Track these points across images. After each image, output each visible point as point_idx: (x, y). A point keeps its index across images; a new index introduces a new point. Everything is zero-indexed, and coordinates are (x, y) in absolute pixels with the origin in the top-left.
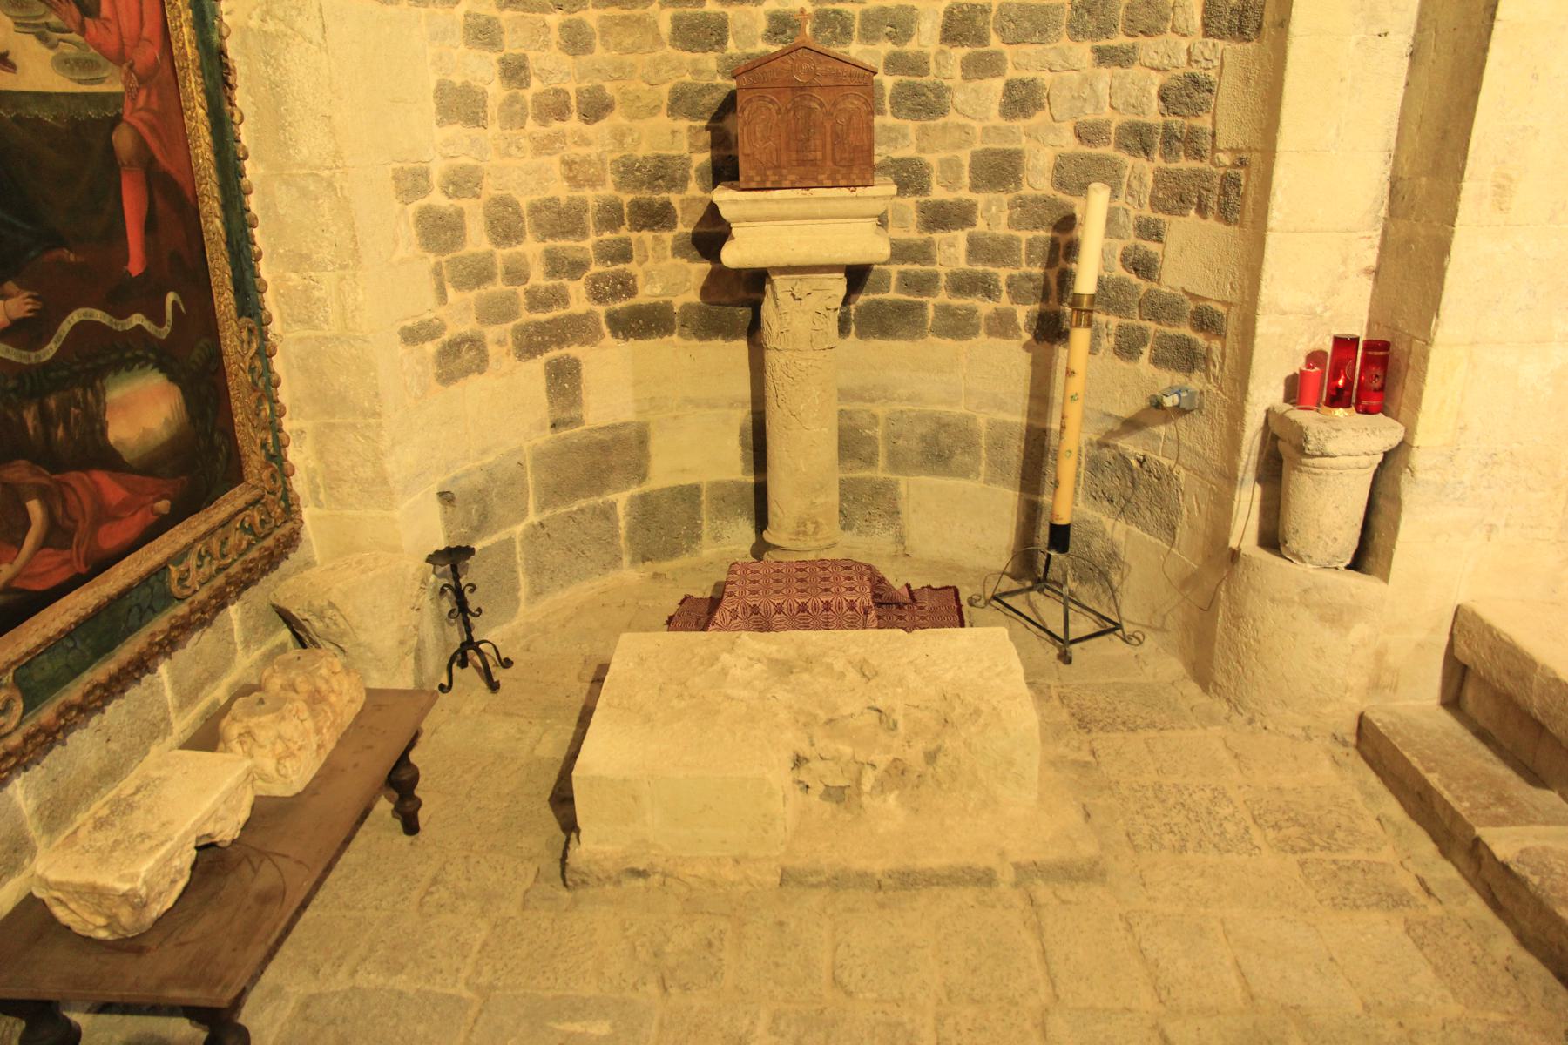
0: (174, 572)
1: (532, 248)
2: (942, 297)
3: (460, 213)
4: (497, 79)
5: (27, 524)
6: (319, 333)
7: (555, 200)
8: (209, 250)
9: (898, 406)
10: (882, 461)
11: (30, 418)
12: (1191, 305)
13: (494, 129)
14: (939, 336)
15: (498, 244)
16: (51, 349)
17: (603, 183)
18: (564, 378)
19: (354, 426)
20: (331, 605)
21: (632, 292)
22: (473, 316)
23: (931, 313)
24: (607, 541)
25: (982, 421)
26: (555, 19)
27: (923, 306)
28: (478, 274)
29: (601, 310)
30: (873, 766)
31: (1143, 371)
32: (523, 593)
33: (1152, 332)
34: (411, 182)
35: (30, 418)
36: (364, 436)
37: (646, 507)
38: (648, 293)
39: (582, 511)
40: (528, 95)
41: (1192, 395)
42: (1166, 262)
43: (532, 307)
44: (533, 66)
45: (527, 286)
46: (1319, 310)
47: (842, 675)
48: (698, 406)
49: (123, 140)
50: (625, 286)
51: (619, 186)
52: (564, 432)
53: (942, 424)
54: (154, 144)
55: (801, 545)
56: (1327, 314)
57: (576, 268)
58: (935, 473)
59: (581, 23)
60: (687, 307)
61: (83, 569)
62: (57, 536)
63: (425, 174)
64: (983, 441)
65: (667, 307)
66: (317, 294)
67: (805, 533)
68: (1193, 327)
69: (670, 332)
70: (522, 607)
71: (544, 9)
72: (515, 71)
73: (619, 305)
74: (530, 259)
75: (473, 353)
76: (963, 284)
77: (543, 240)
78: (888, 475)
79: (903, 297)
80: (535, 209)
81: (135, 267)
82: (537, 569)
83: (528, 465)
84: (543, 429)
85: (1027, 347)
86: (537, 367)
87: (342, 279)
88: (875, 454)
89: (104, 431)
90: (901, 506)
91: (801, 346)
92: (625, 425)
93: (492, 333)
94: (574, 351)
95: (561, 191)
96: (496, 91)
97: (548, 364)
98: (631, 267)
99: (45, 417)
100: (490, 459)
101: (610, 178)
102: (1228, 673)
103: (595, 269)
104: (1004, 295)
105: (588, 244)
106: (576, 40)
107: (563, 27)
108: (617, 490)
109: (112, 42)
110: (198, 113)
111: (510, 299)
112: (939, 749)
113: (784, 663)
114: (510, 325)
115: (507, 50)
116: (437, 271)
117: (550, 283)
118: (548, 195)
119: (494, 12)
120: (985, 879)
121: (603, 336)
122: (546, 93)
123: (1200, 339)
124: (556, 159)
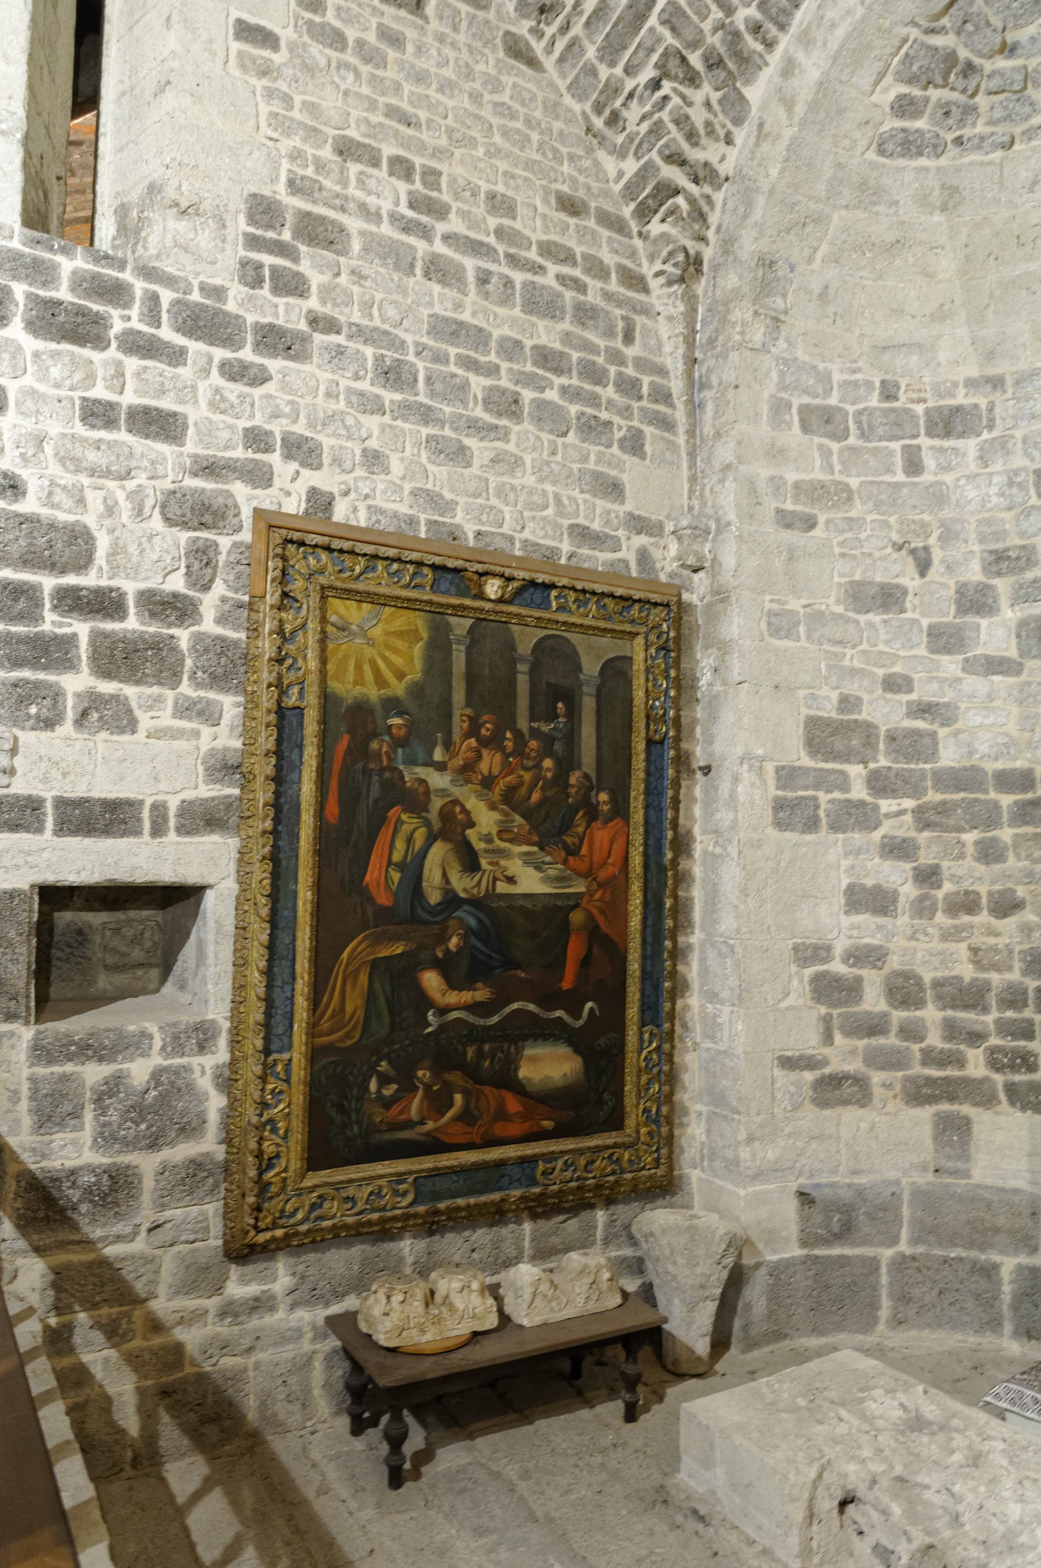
0: (541, 1167)
1: (931, 1014)
3: (859, 980)
4: (910, 882)
5: (451, 1105)
7: (959, 978)
8: (630, 981)
11: (470, 1052)
13: (903, 920)
15: (896, 1008)
16: (495, 1019)
17: (1010, 969)
18: (954, 1132)
24: (989, 1301)
26: (970, 837)
28: (874, 1027)
29: (999, 1079)
34: (811, 953)
35: (470, 1052)
39: (961, 1260)
40: (940, 894)
43: (924, 1063)
44: (945, 874)
49: (577, 917)
51: (1025, 972)
52: (948, 1180)
54: (600, 919)
57: (975, 1037)
59: (995, 840)
61: (478, 1141)
62: (467, 1117)
63: (828, 949)
70: (881, 1327)
71: (960, 830)
72: (928, 876)
73: (1018, 1078)
74: (928, 1024)
80: (937, 984)
81: (566, 984)
82: (902, 1298)
86: (926, 1113)
89: (516, 1070)
92: (1016, 1191)
93: (877, 1077)
94: (966, 1109)
95: (967, 972)
96: (908, 891)
98: (1033, 1046)
99: (479, 1053)
100: (862, 1180)
101: (1017, 965)
103: (994, 1041)
105: (990, 1019)
106: (990, 853)
107: (977, 843)
108: (1002, 1252)
109: (583, 867)
110: (636, 900)
114: (900, 1074)
115: (921, 861)
116: (827, 1020)
117: (947, 1046)
118: (954, 973)
119: (913, 834)
121: (999, 1102)
122: (957, 893)
124: (964, 946)
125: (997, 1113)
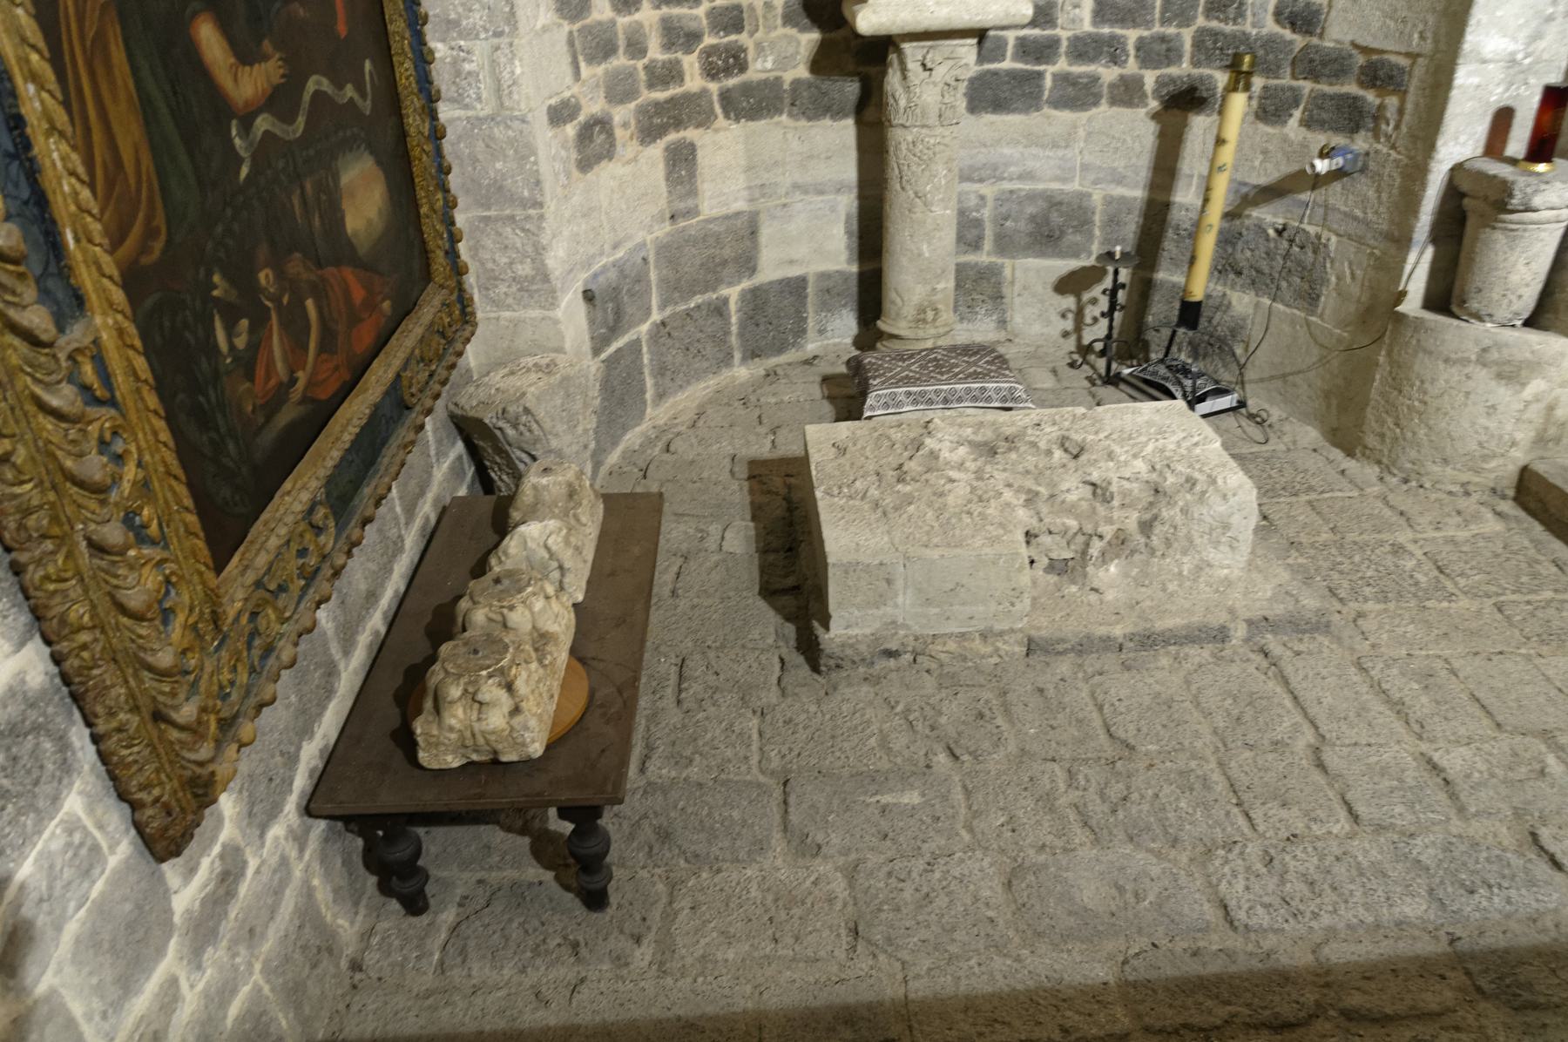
2: (1062, 65)
6: (470, 113)
9: (1007, 186)
10: (988, 244)
12: (1361, 60)
14: (1056, 108)
19: (512, 218)
20: (527, 411)
21: (743, 68)
22: (602, 95)
23: (1048, 82)
24: (721, 339)
25: (1097, 197)
27: (1040, 75)
28: (599, 45)
29: (714, 87)
30: (1101, 537)
31: (1292, 135)
32: (649, 396)
33: (1306, 91)
36: (523, 230)
37: (756, 300)
38: (760, 68)
39: (698, 307)
41: (1357, 156)
42: (1333, 13)
43: (651, 86)
45: (646, 61)
46: (1520, 56)
47: (1049, 453)
48: (806, 192)
50: (735, 60)
52: (682, 224)
53: (1053, 202)
55: (921, 334)
56: (1527, 61)
57: (691, 38)
58: (1042, 255)
60: (796, 83)
64: (1097, 218)
65: (778, 80)
66: (467, 67)
67: (924, 321)
68: (1361, 84)
69: (780, 112)
70: (649, 410)
73: (732, 82)
75: (603, 137)
76: (1084, 49)
77: (658, 7)
78: (993, 259)
79: (1020, 66)
82: (661, 371)
83: (652, 259)
84: (663, 221)
85: (1155, 116)
86: (657, 151)
87: (498, 48)
88: (980, 238)
90: (1006, 290)
91: (930, 122)
92: (738, 214)
94: (690, 134)
97: (667, 149)
98: (743, 38)
102: (1382, 436)
103: (709, 40)
104: (1131, 60)
108: (730, 284)
111: (631, 74)
112: (1155, 518)
113: (985, 444)
114: (632, 105)
117: (666, 57)
120: (1220, 635)
123: (1371, 97)
125: (717, 131)
